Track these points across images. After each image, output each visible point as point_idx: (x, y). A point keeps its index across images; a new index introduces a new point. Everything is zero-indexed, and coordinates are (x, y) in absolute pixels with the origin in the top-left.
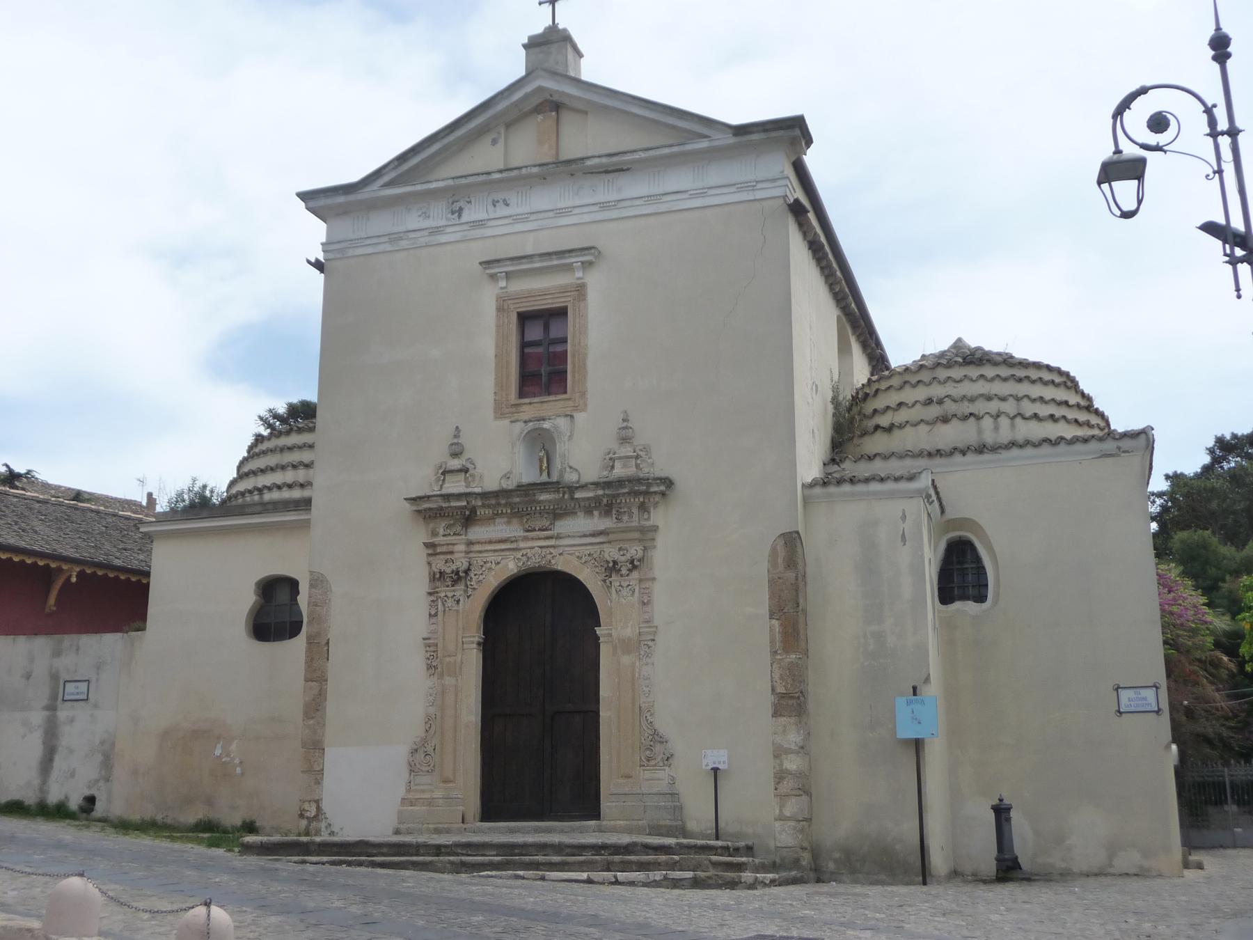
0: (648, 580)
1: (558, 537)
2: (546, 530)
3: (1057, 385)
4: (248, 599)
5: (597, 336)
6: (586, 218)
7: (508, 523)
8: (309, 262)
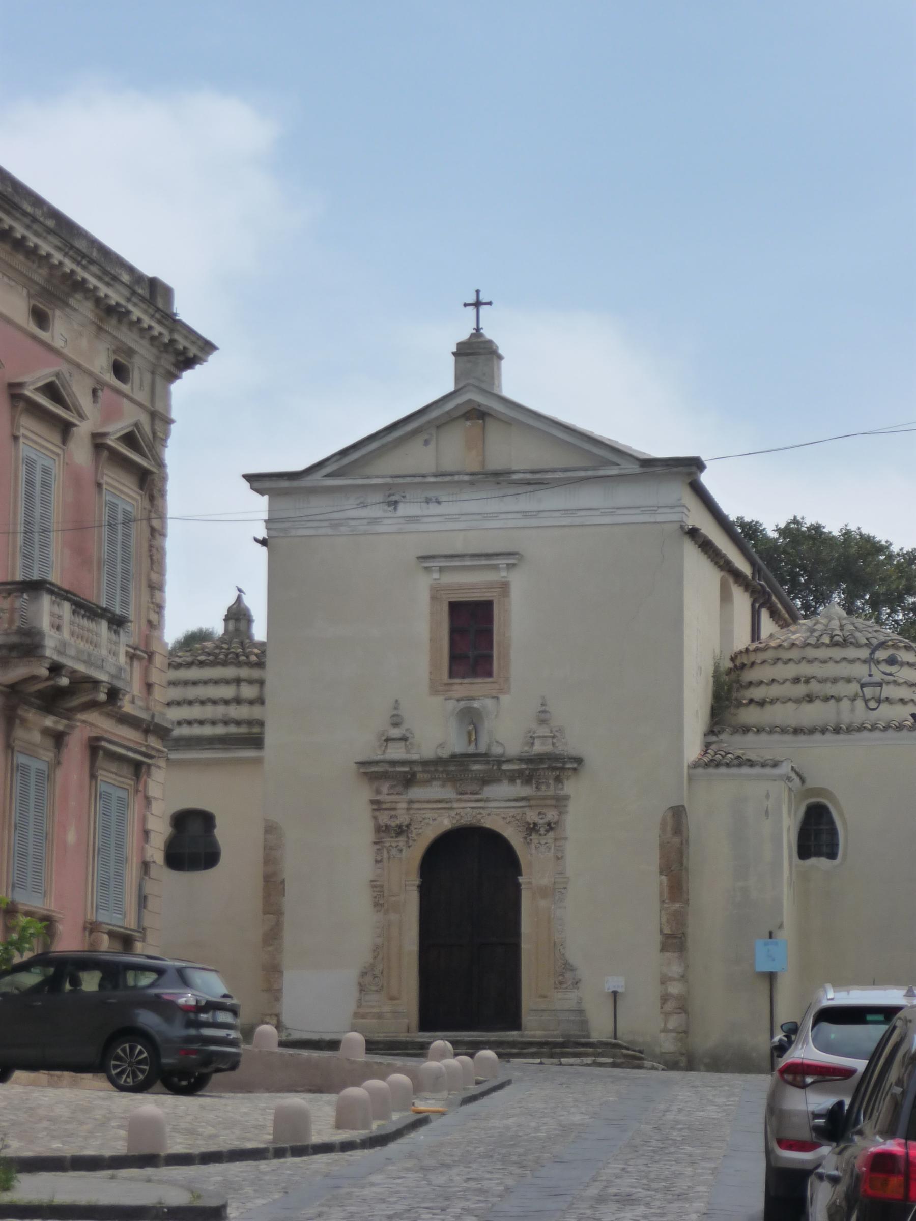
1: (487, 800)
2: (477, 793)
5: (518, 628)
6: (511, 524)
7: (443, 786)
8: (256, 540)
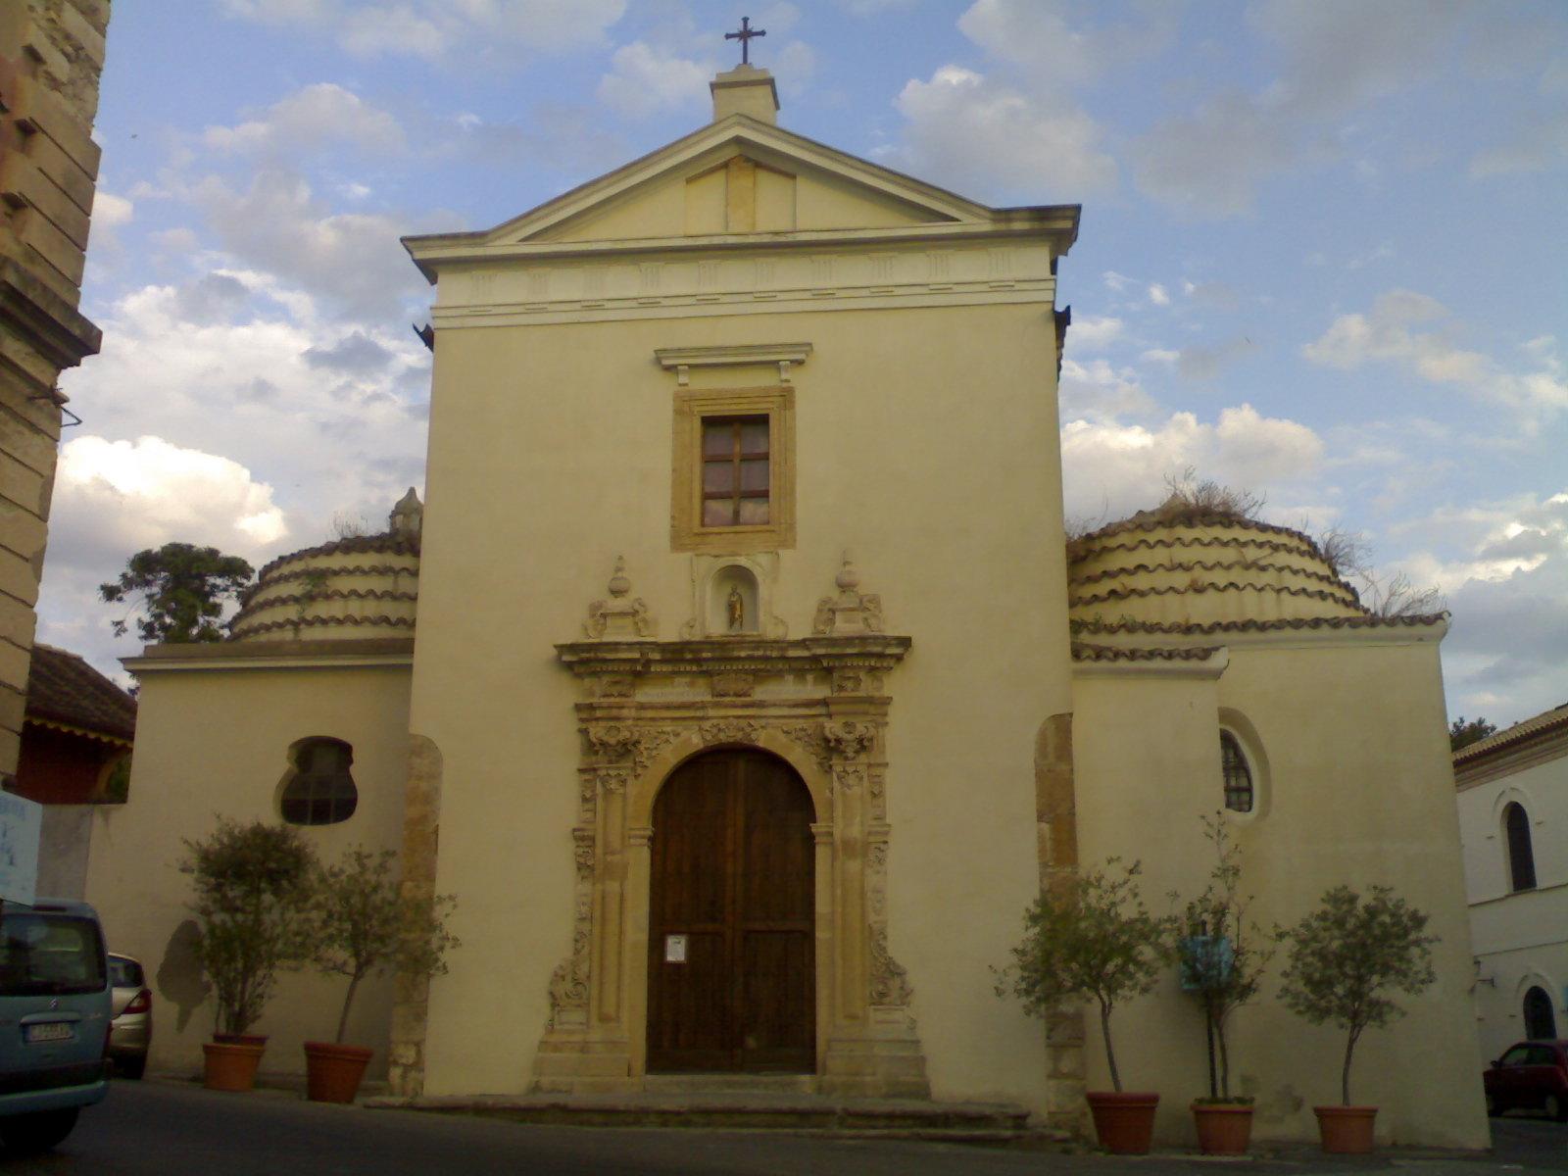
0: (879, 765)
1: (761, 705)
2: (745, 695)
3: (1302, 554)
4: (279, 766)
7: (692, 684)
8: (415, 328)
